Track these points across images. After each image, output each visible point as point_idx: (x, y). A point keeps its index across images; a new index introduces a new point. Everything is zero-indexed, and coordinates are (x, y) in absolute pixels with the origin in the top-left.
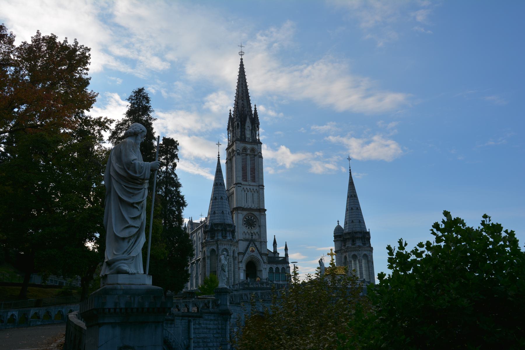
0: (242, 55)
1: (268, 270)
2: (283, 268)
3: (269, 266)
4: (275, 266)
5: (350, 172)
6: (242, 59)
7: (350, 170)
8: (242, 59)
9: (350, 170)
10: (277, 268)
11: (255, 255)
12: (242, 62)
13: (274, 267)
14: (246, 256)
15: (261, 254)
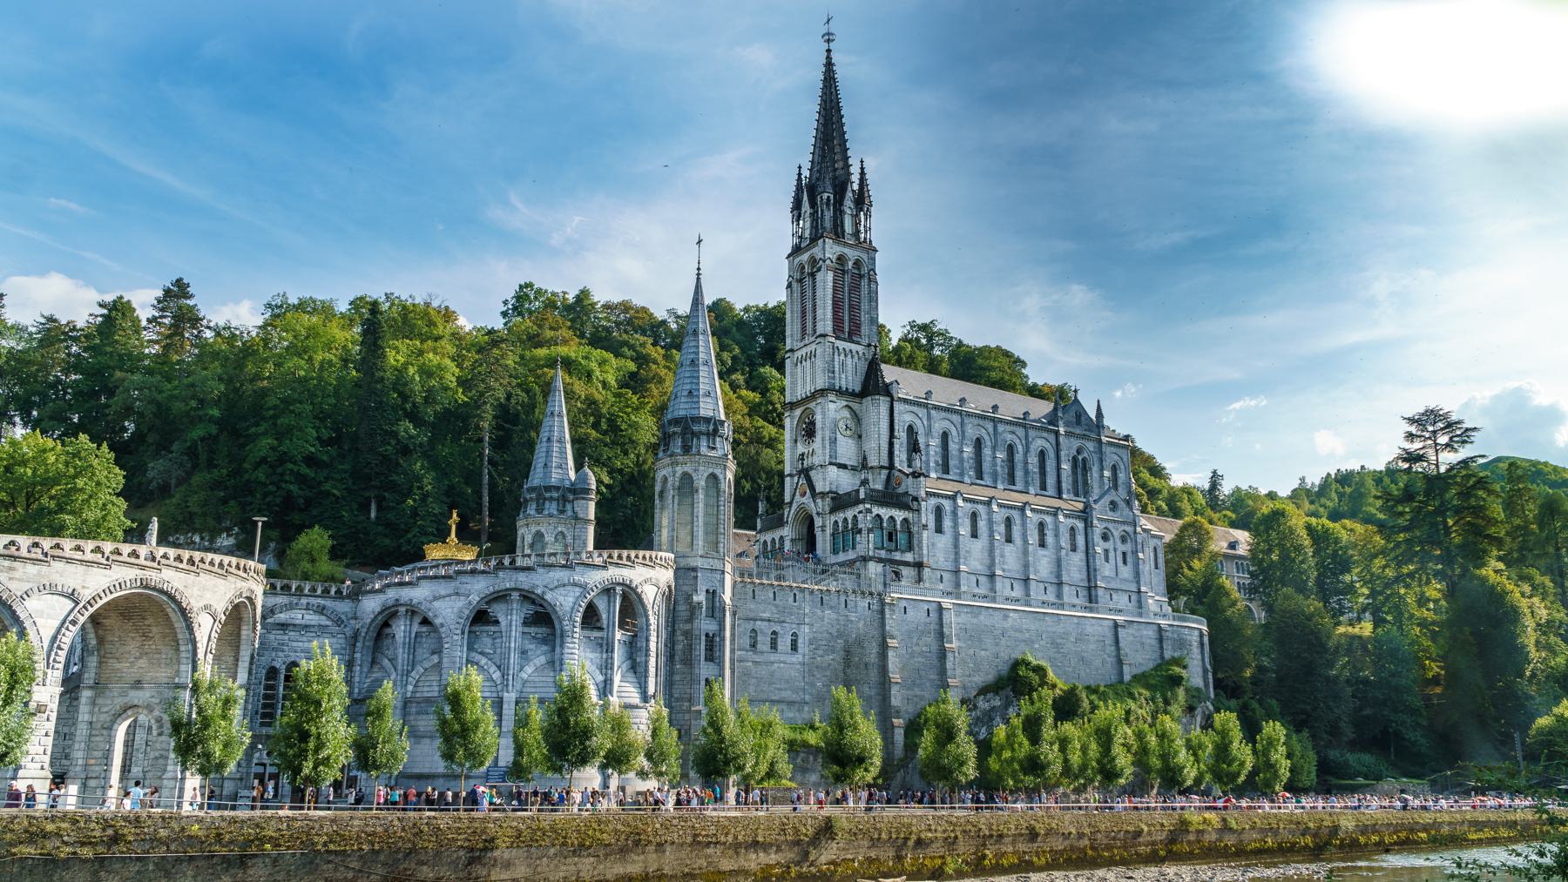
0: (828, 41)
1: (829, 531)
2: (855, 516)
3: (833, 518)
4: (842, 515)
5: (698, 274)
6: (829, 51)
7: (699, 269)
8: (829, 51)
9: (699, 269)
10: (845, 519)
11: (806, 501)
12: (829, 58)
13: (840, 516)
14: (794, 506)
15: (814, 494)
